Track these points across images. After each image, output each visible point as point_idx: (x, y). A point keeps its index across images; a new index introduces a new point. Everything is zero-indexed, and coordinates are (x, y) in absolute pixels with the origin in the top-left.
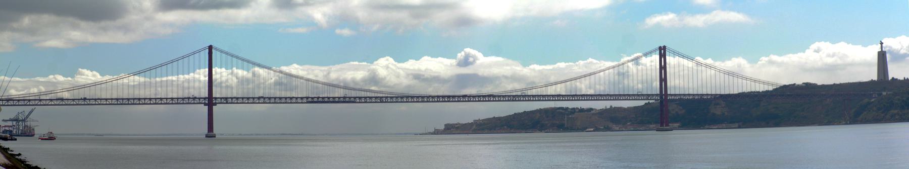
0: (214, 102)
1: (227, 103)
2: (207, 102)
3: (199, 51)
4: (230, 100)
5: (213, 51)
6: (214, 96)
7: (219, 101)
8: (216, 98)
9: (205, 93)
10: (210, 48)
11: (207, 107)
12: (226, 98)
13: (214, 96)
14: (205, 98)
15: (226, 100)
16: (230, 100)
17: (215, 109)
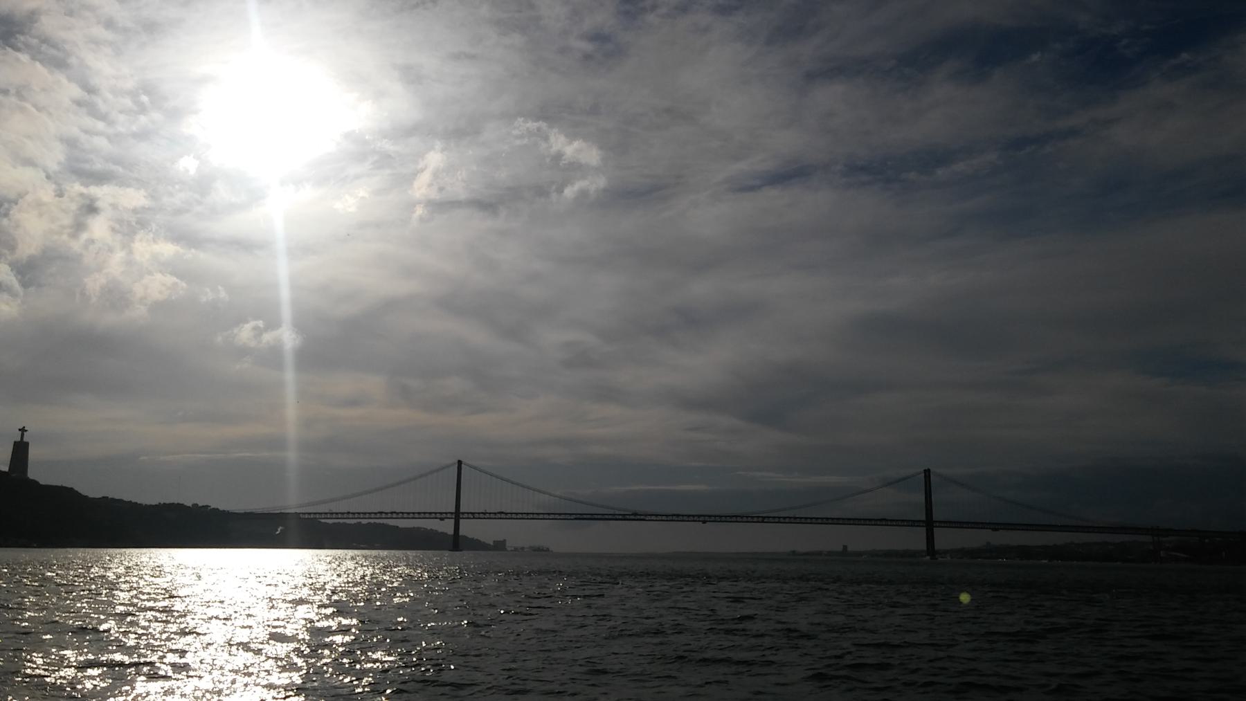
0: (461, 516)
1: (474, 518)
2: (454, 517)
3: (448, 466)
4: (477, 516)
5: (463, 465)
6: (461, 511)
7: (466, 516)
8: (463, 513)
9: (453, 510)
10: (460, 463)
11: (453, 521)
12: (473, 513)
13: (461, 511)
14: (452, 513)
15: (473, 515)
16: (477, 516)
17: (461, 521)
